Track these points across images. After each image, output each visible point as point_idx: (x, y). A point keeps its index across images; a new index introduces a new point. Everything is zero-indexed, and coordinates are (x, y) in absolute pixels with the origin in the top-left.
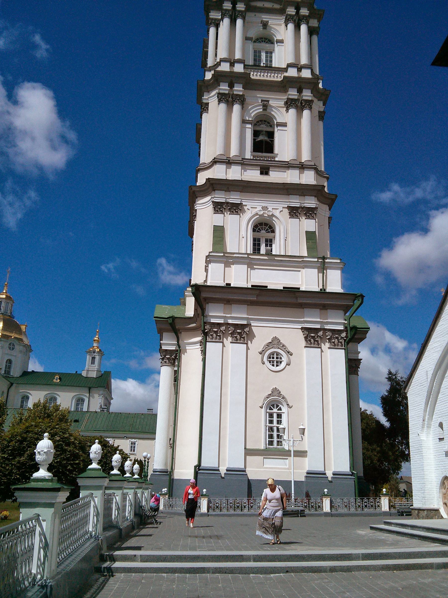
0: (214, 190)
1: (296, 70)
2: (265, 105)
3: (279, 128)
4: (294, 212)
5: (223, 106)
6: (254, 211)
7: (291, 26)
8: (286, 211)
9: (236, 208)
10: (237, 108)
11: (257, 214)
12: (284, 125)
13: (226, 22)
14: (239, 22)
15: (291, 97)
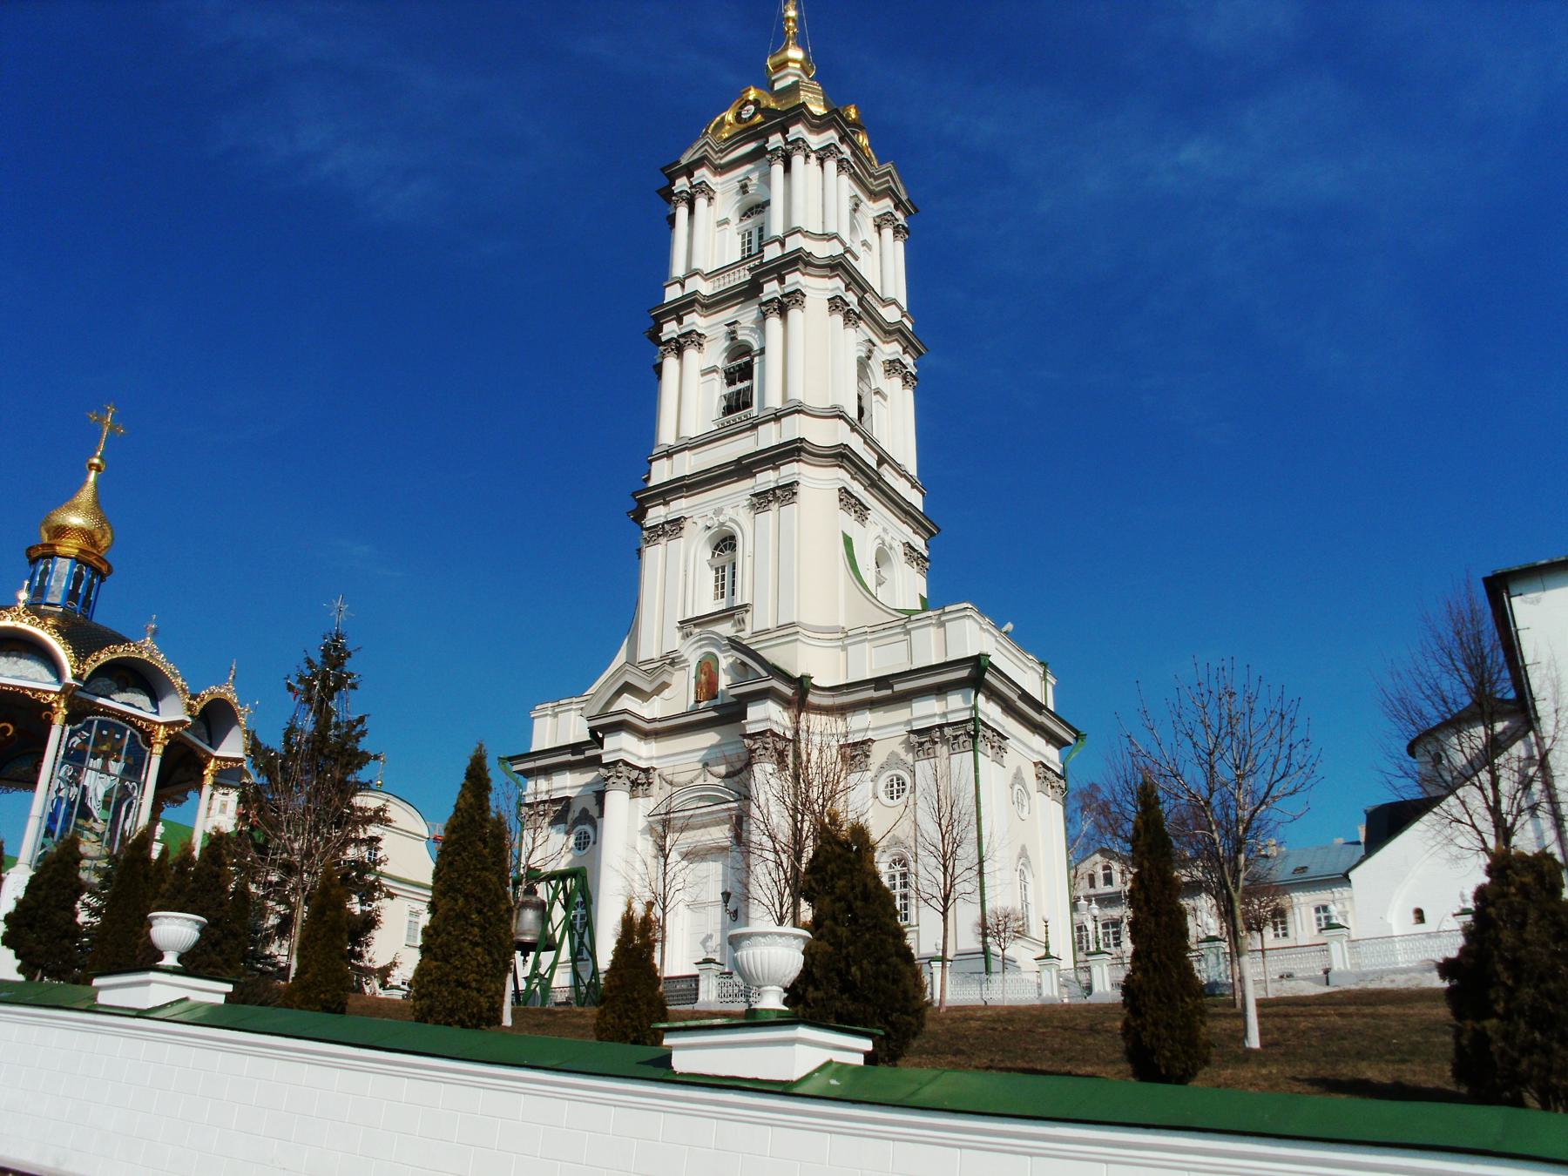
7: (888, 232)
9: (861, 510)
12: (884, 397)
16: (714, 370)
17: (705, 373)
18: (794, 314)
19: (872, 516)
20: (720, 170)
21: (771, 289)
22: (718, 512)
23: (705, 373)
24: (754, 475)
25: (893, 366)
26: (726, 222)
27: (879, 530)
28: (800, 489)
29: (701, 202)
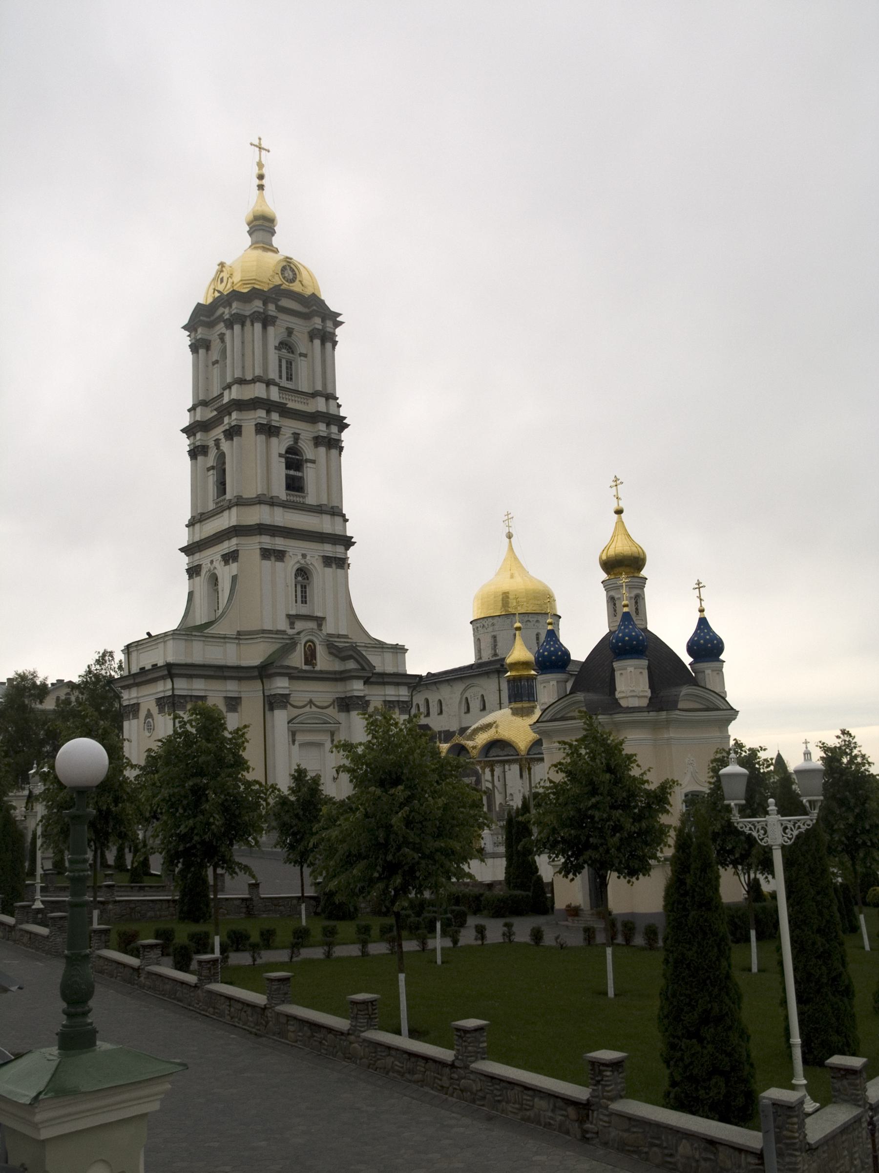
0: (261, 534)
1: (324, 399)
2: (296, 436)
3: (309, 465)
4: (328, 561)
5: (262, 438)
6: (296, 560)
7: (317, 342)
8: (320, 560)
9: (280, 555)
10: (274, 440)
11: (298, 562)
12: (313, 462)
13: (258, 326)
14: (271, 330)
15: (322, 434)
16: (213, 468)
17: (208, 469)
18: (235, 439)
19: (291, 552)
20: (211, 325)
21: (226, 420)
22: (212, 562)
23: (208, 469)
24: (222, 542)
25: (318, 441)
26: (217, 362)
27: (300, 557)
28: (240, 552)
29: (202, 351)
